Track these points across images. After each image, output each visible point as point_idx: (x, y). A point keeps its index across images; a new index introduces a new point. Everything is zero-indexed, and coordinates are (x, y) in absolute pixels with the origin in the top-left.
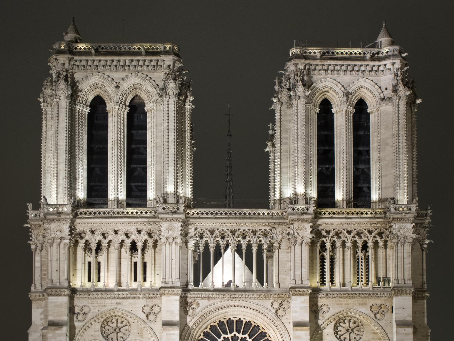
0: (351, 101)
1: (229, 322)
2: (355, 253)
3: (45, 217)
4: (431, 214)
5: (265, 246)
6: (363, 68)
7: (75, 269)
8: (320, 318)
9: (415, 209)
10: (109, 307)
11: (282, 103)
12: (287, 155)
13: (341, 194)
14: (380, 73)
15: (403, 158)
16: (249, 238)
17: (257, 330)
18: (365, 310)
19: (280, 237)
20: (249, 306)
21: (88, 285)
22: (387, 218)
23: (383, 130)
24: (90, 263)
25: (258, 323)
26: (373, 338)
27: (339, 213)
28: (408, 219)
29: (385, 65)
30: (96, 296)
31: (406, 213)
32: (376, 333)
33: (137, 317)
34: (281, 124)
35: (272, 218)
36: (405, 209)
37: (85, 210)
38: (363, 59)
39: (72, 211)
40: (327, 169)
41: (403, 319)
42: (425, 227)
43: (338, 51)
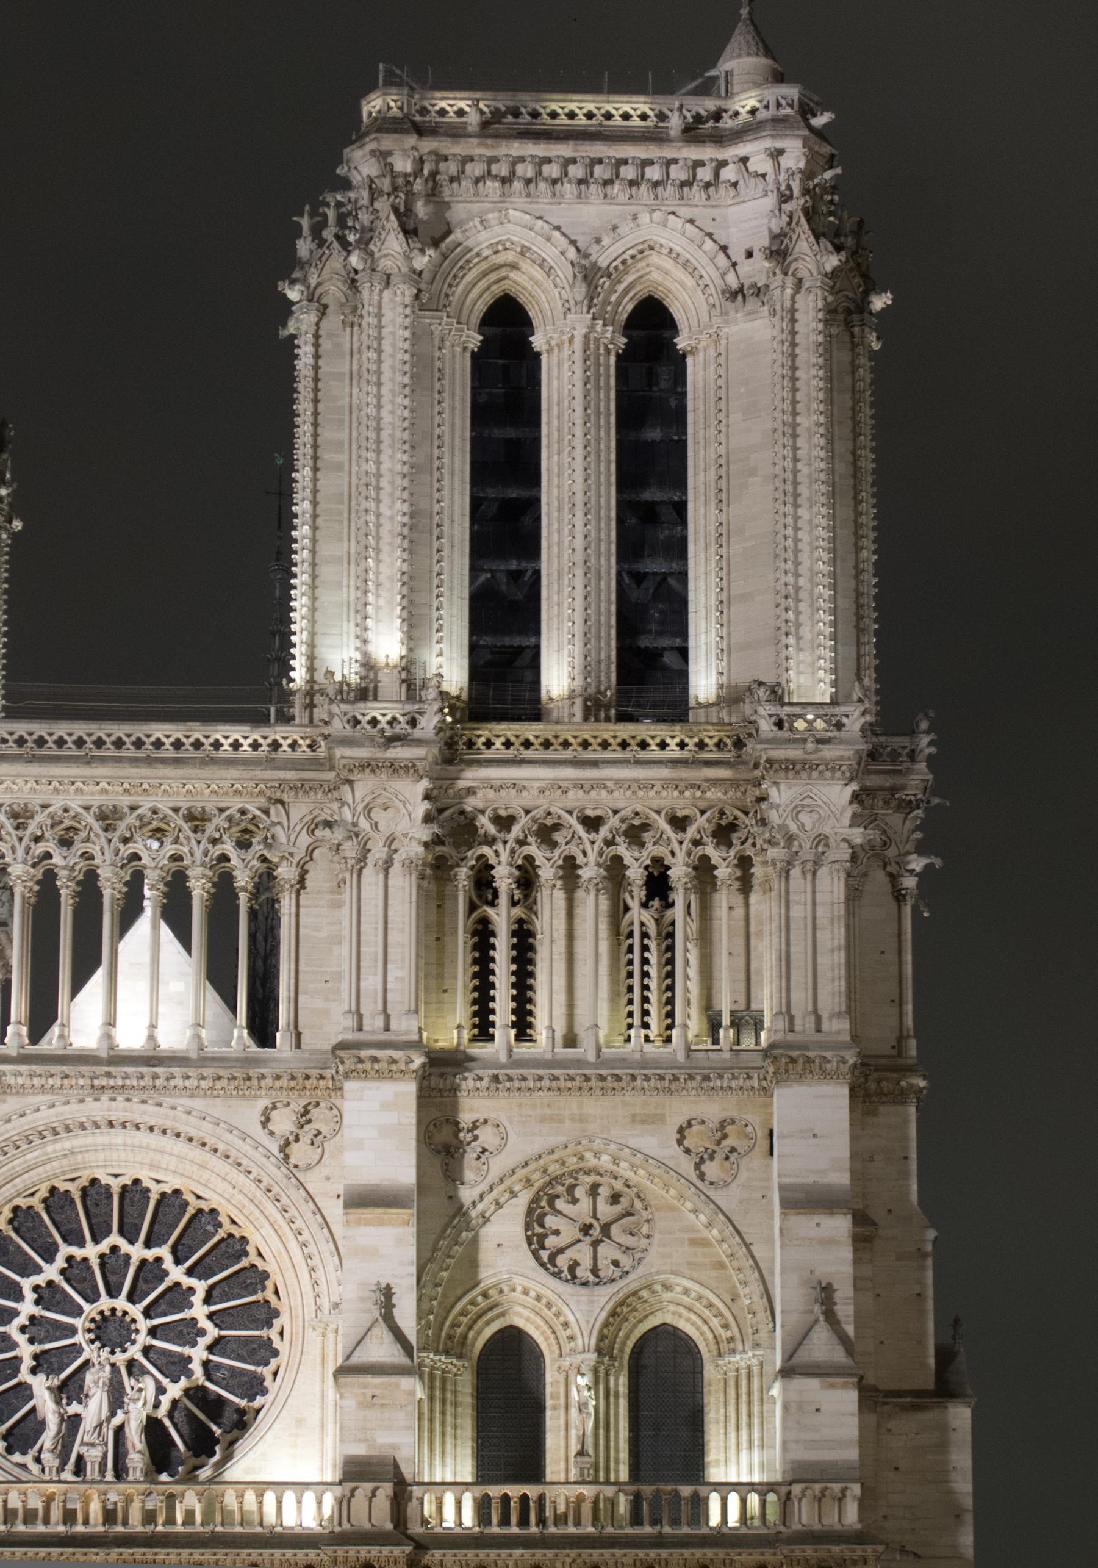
0: (606, 302)
1: (92, 1192)
2: (619, 909)
4: (932, 750)
5: (243, 879)
6: (654, 173)
8: (469, 1175)
9: (857, 727)
11: (326, 307)
12: (340, 513)
13: (566, 670)
14: (723, 193)
15: (810, 522)
16: (176, 841)
17: (210, 1228)
18: (658, 1143)
19: (305, 840)
22: (745, 763)
23: (735, 417)
25: (213, 1200)
26: (689, 1264)
27: (547, 744)
28: (832, 767)
29: (744, 160)
31: (821, 741)
32: (704, 1243)
34: (316, 390)
35: (269, 763)
36: (820, 724)
38: (655, 136)
40: (515, 576)
42: (907, 806)
43: (554, 106)
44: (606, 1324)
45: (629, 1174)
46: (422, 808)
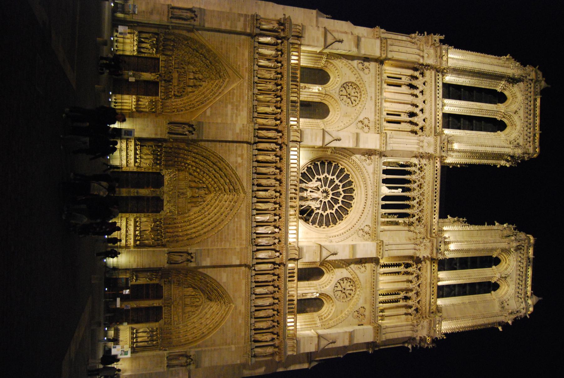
8: (356, 266)
10: (368, 91)
18: (361, 303)
24: (400, 79)
45: (355, 297)
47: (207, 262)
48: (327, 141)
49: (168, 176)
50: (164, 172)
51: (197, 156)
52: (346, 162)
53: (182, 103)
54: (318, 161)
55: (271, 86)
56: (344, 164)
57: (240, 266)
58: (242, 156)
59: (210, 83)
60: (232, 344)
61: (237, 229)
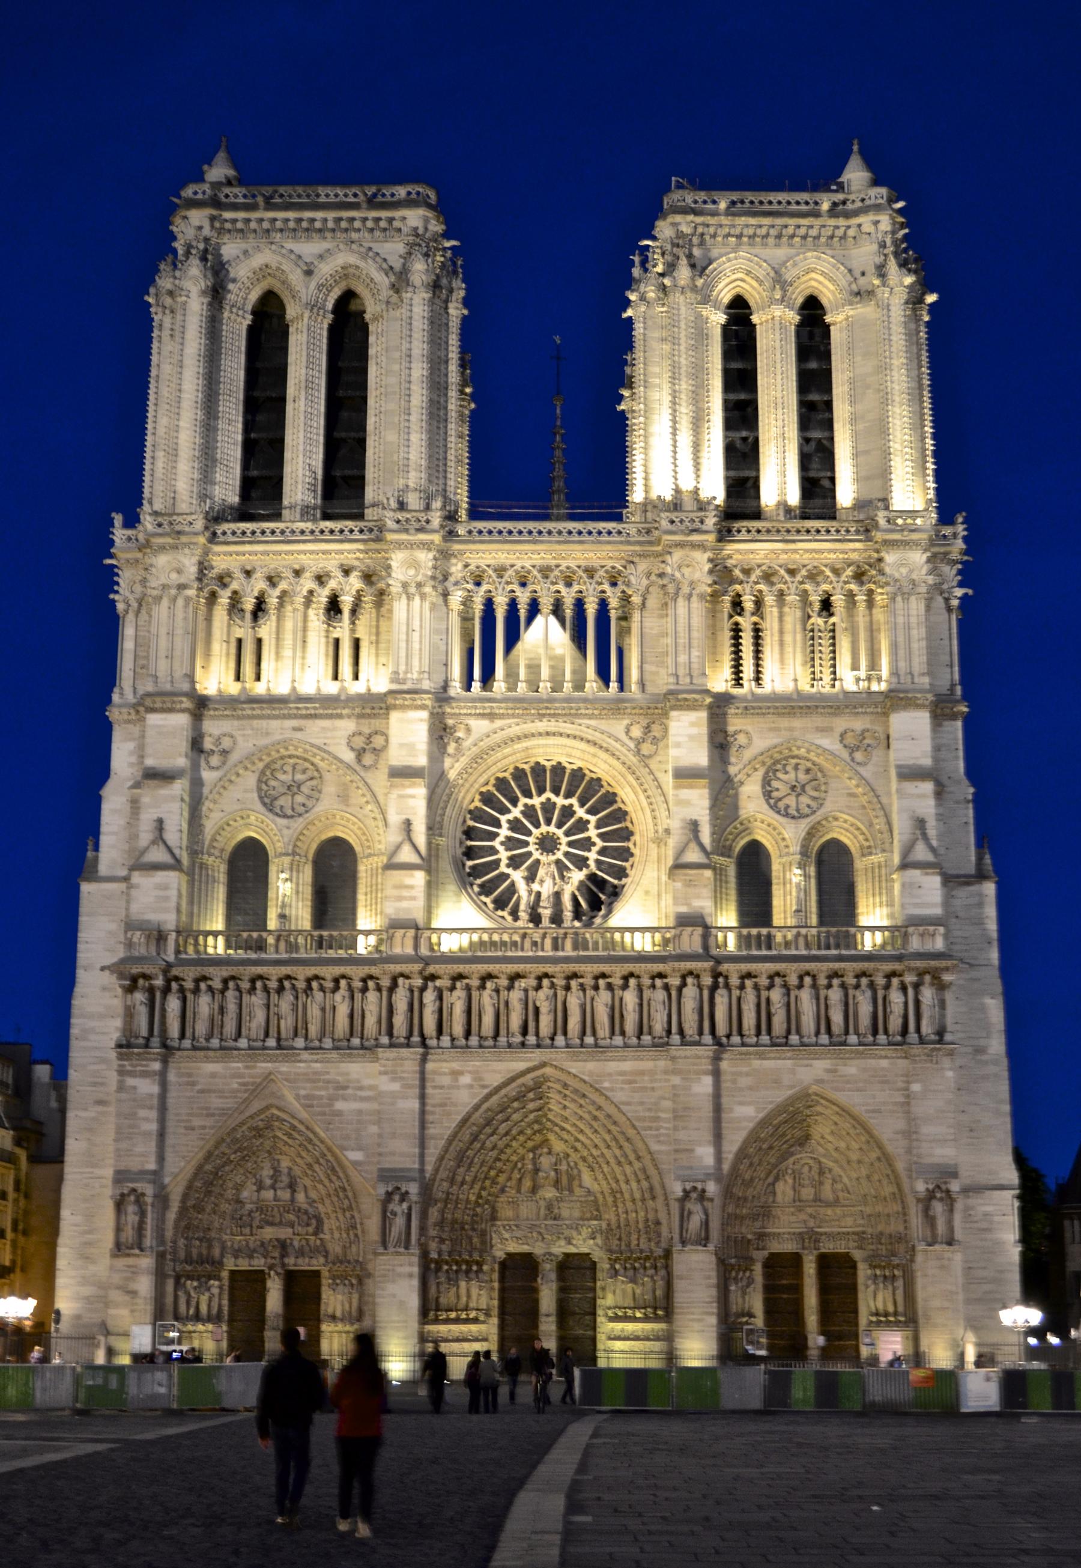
3: (148, 541)
7: (208, 654)
8: (733, 760)
10: (278, 737)
18: (831, 743)
20: (578, 733)
21: (233, 689)
24: (240, 641)
25: (600, 774)
30: (249, 712)
33: (336, 758)
37: (233, 526)
39: (206, 528)
41: (911, 762)
44: (805, 839)
46: (708, 566)
47: (706, 1154)
48: (414, 859)
49: (507, 1243)
50: (500, 1254)
51: (459, 1179)
52: (463, 791)
53: (333, 1216)
54: (464, 865)
55: (285, 1004)
56: (469, 797)
57: (716, 1074)
58: (456, 1074)
59: (286, 1149)
60: (907, 1089)
61: (630, 1082)
